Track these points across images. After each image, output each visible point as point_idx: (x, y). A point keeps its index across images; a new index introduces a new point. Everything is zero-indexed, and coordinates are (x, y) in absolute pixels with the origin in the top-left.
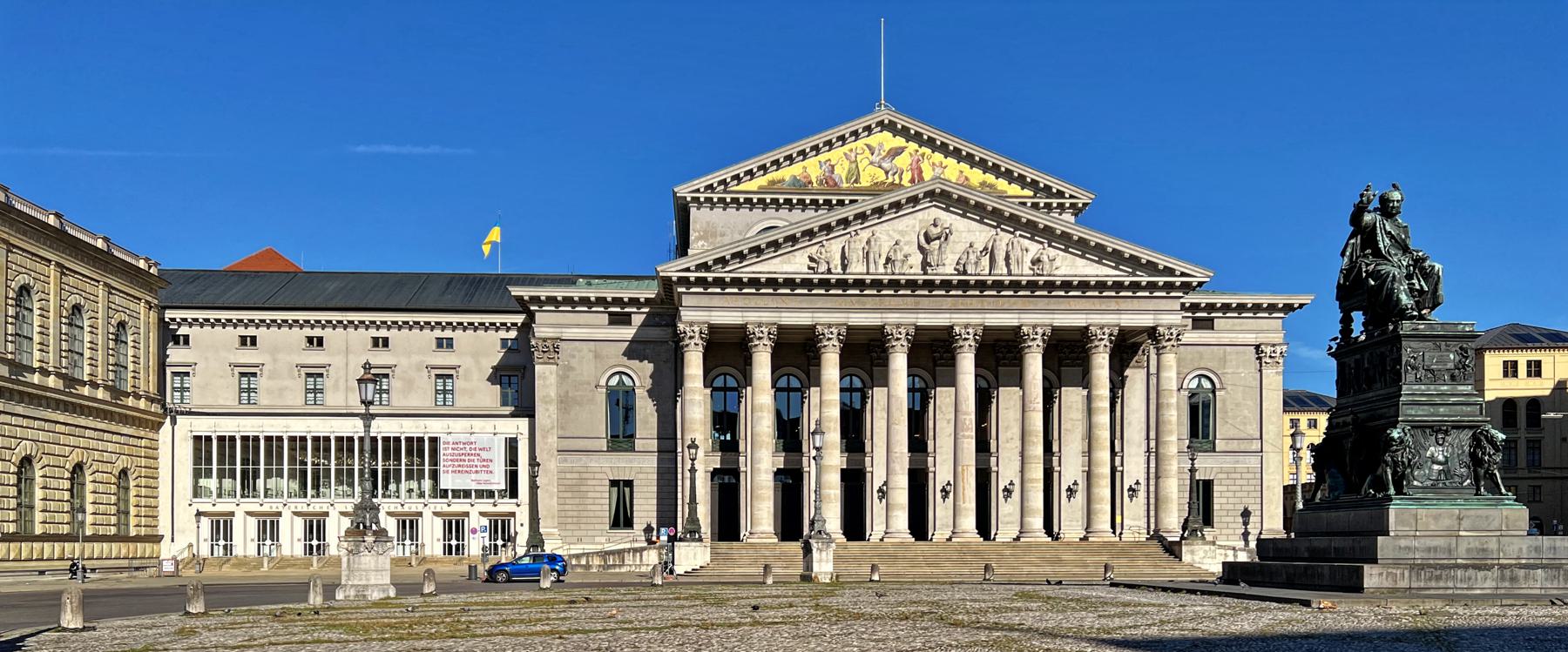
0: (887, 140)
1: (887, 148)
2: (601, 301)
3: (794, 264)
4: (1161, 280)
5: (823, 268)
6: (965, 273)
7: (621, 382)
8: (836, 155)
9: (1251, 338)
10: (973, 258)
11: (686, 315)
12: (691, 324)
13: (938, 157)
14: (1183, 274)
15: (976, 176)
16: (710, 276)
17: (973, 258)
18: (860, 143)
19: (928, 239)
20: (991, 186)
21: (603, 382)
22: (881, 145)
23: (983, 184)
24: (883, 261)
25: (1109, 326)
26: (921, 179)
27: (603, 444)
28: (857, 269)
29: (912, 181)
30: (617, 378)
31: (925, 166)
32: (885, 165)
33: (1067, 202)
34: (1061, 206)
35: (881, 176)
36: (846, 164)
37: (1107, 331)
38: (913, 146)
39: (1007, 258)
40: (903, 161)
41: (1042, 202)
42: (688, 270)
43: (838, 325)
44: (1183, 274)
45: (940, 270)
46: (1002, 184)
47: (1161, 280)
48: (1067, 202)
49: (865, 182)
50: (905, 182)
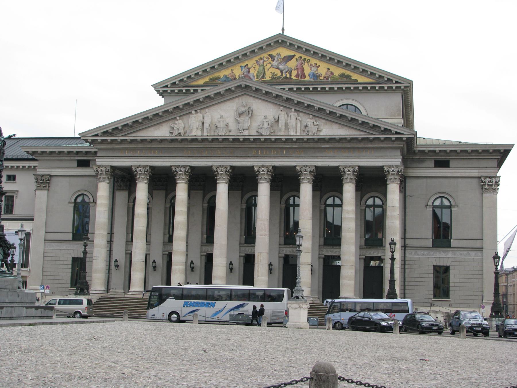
0: (285, 52)
1: (282, 56)
2: (69, 153)
3: (162, 132)
4: (382, 137)
5: (176, 133)
6: (261, 135)
7: (83, 200)
8: (251, 63)
9: (475, 172)
10: (266, 125)
11: (99, 161)
12: (102, 166)
13: (313, 61)
14: (397, 133)
15: (337, 71)
16: (109, 138)
17: (266, 125)
18: (266, 55)
19: (240, 115)
20: (348, 77)
21: (73, 200)
22: (279, 54)
23: (342, 75)
24: (214, 128)
25: (352, 166)
26: (304, 76)
27: (70, 237)
28: (196, 133)
29: (297, 76)
30: (82, 197)
31: (306, 67)
32: (281, 67)
33: (394, 86)
35: (279, 74)
36: (257, 67)
37: (351, 169)
38: (298, 55)
39: (286, 125)
40: (292, 64)
41: (377, 86)
42: (97, 135)
43: (184, 166)
44: (397, 133)
45: (246, 133)
46: (355, 76)
47: (382, 137)
48: (394, 86)
49: (268, 77)
50: (293, 77)
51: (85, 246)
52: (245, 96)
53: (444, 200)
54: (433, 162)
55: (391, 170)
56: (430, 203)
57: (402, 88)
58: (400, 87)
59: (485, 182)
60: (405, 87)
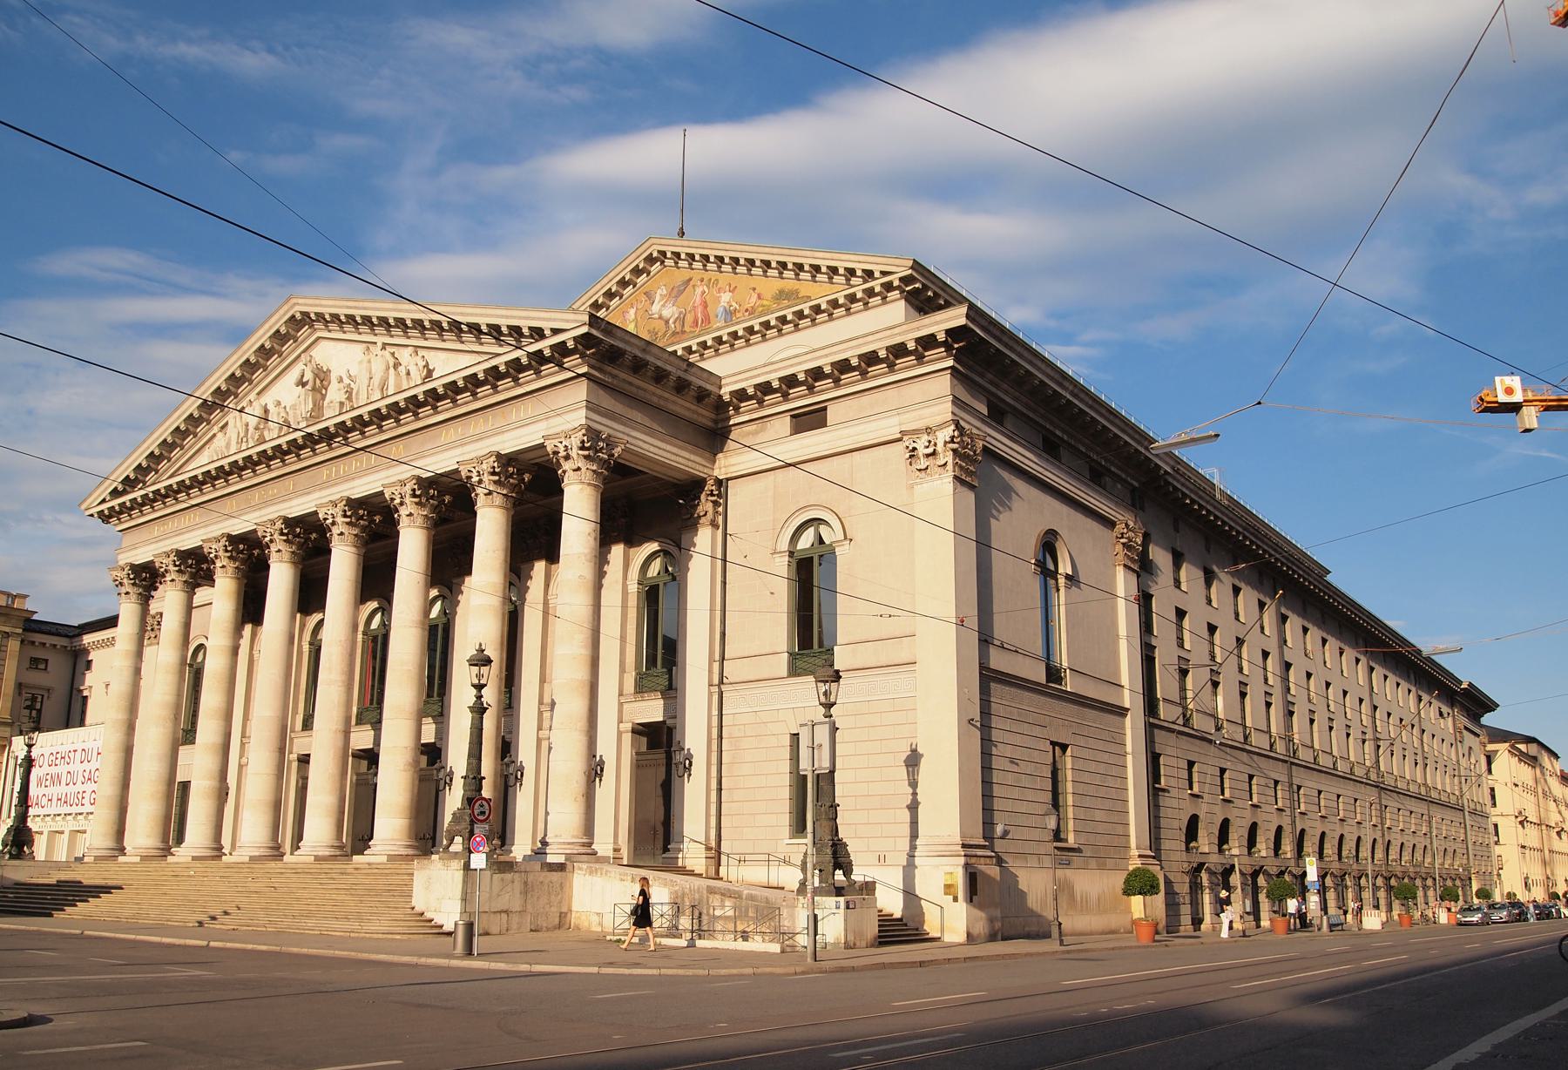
3: (203, 463)
23: (782, 295)
33: (876, 285)
34: (870, 293)
42: (104, 501)
44: (555, 331)
46: (805, 286)
48: (876, 285)
51: (30, 746)
52: (323, 343)
53: (823, 529)
54: (787, 419)
55: (561, 449)
56: (784, 545)
57: (896, 283)
58: (890, 283)
59: (914, 449)
60: (905, 280)
